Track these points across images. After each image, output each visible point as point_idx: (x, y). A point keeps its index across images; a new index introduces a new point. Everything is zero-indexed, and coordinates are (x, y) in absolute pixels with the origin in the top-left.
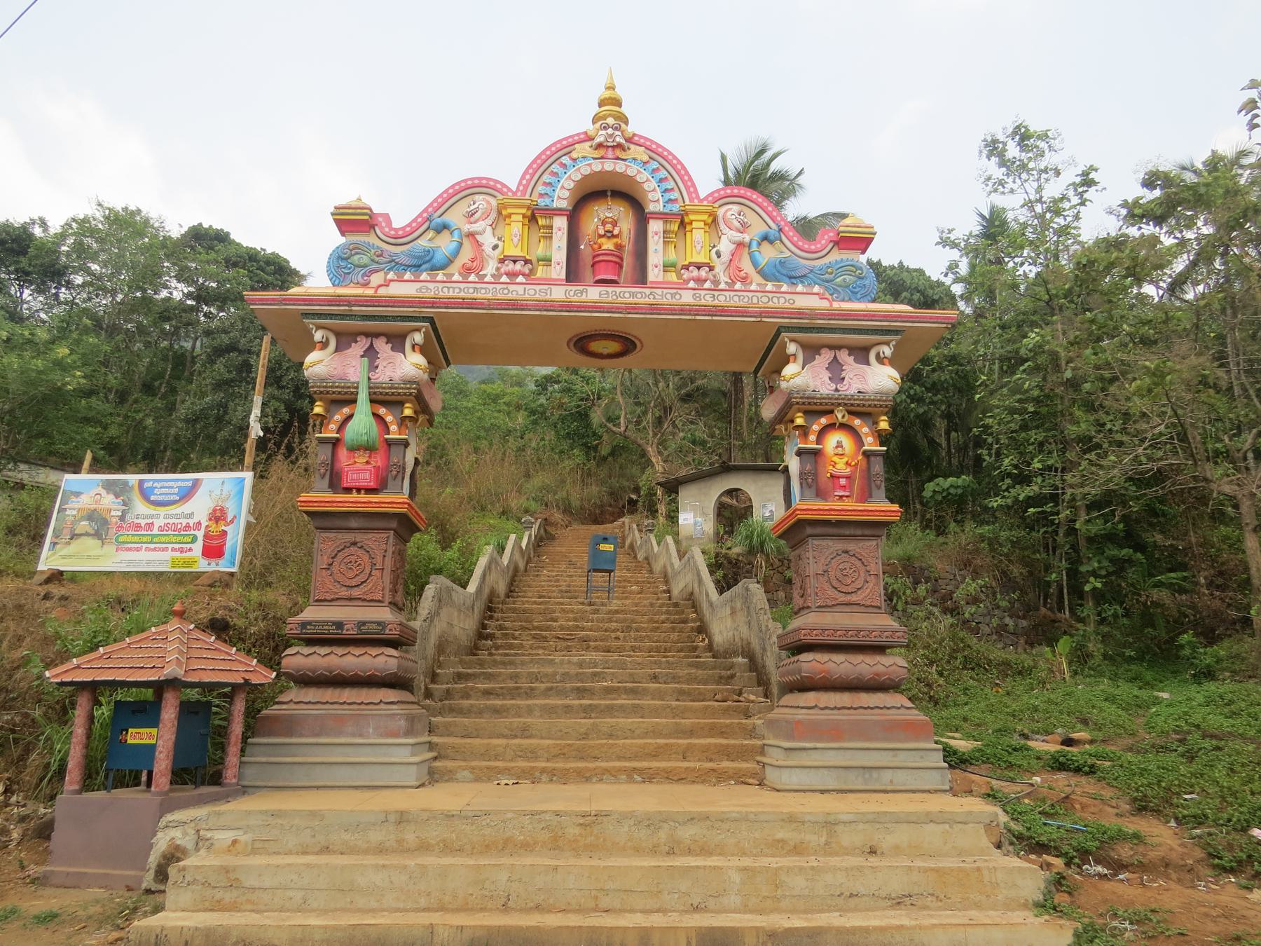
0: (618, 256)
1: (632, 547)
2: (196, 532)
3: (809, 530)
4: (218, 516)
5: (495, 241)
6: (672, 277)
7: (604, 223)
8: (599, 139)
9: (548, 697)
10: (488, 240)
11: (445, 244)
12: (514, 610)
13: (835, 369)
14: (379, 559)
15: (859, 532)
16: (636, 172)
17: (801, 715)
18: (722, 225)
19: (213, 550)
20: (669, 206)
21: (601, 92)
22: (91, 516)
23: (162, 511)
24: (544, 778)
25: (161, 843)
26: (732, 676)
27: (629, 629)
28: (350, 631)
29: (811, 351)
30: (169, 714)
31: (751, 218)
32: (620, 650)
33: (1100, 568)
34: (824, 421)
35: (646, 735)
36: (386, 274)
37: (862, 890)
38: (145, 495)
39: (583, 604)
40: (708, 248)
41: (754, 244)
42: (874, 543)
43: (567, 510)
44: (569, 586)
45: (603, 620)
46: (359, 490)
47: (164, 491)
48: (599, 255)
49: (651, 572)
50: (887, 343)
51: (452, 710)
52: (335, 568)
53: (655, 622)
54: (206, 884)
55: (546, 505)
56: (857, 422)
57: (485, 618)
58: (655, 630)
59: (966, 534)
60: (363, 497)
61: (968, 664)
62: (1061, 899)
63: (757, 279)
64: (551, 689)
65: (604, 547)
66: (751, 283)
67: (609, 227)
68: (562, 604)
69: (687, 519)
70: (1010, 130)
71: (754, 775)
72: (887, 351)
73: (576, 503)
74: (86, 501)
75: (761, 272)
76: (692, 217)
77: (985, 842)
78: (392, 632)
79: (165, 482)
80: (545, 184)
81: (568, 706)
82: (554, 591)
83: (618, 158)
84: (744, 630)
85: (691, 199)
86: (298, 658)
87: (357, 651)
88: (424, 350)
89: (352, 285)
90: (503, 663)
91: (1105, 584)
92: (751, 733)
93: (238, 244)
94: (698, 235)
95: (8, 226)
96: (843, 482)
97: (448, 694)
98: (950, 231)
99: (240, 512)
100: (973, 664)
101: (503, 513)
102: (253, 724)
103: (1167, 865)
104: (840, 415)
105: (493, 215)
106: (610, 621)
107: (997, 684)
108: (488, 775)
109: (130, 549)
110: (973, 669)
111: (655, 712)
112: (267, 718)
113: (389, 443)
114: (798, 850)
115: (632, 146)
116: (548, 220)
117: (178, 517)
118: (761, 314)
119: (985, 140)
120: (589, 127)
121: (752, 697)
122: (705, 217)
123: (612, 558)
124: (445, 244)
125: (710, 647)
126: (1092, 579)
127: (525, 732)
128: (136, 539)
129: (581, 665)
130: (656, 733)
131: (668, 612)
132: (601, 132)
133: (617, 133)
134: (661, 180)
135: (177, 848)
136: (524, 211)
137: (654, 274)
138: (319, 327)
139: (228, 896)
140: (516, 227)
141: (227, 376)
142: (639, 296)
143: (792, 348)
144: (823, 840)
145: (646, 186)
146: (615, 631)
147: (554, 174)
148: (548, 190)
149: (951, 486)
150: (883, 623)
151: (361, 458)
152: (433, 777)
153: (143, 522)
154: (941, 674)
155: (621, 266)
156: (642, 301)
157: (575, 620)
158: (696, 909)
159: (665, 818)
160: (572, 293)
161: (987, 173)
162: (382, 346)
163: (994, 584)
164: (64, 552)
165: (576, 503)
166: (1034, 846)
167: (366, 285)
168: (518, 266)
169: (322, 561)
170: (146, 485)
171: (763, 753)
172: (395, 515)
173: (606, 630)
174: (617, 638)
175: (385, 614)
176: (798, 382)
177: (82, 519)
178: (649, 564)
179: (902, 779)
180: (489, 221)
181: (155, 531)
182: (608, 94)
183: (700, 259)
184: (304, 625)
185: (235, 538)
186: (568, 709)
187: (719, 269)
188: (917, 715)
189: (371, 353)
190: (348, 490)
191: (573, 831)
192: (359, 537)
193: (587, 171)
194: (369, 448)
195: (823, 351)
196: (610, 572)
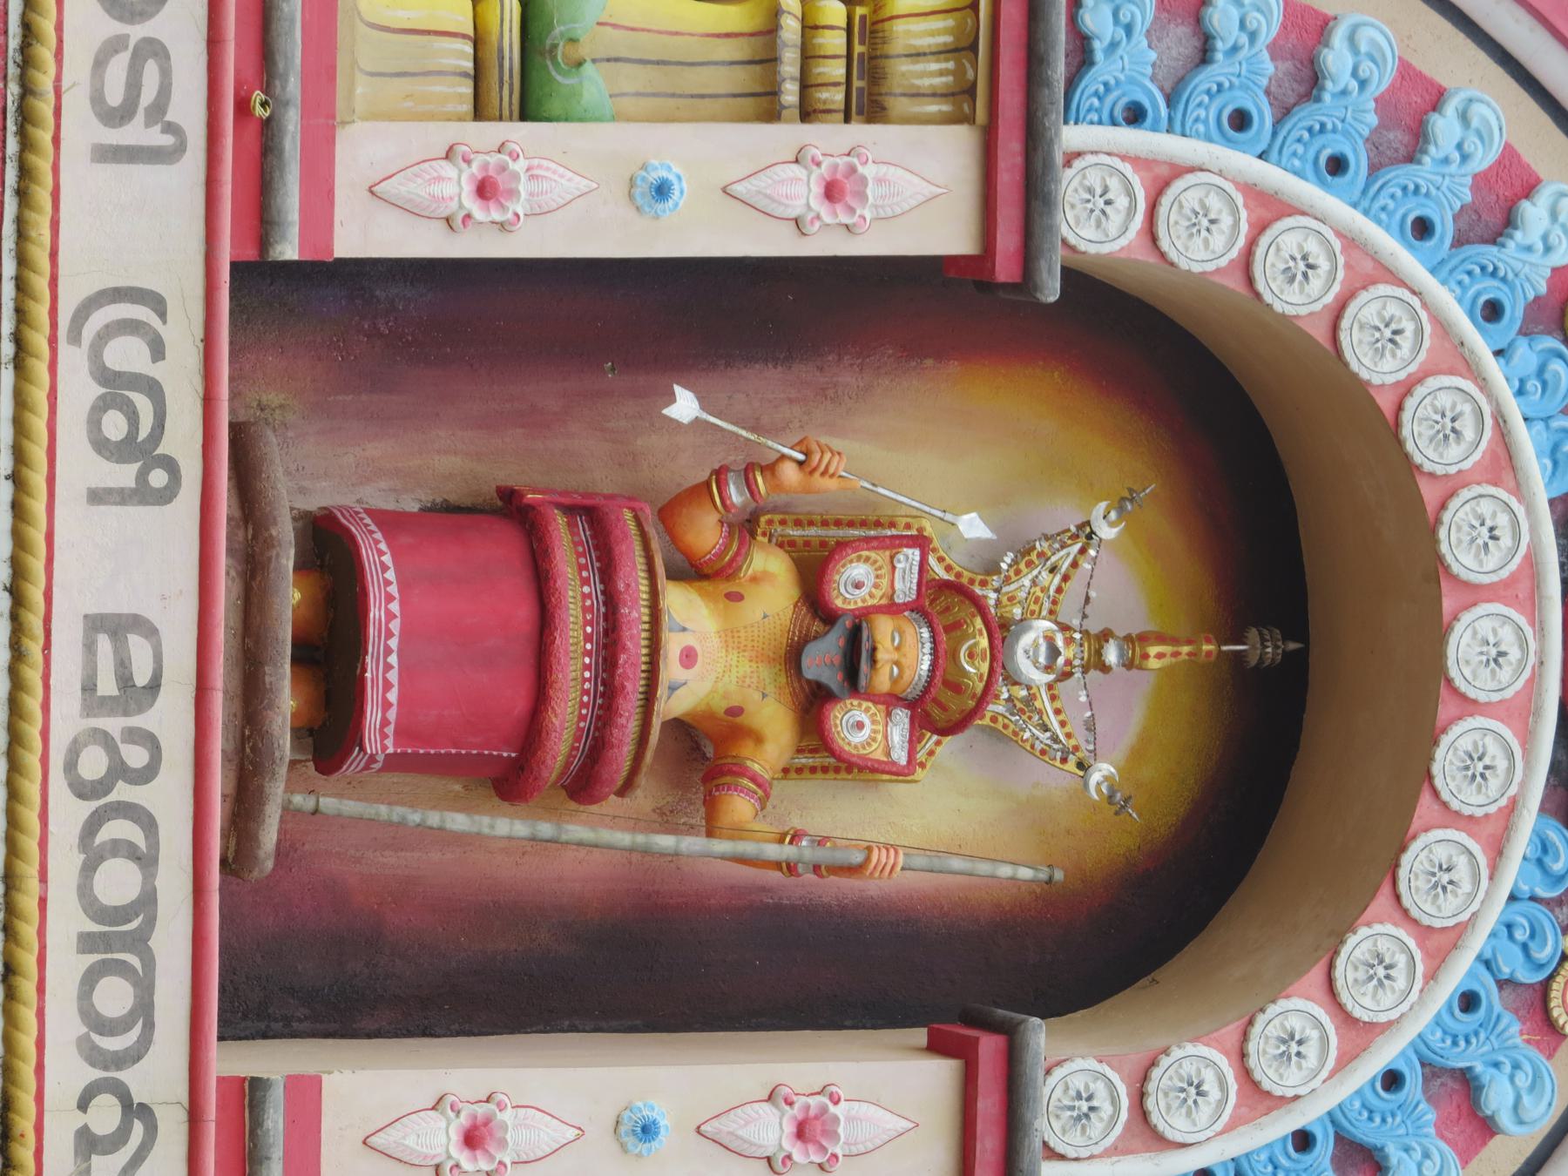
0: (596, 747)
16: (1439, 912)
48: (607, 568)
116: (933, 74)
142: (114, 997)
156: (64, 1025)
160: (127, 355)
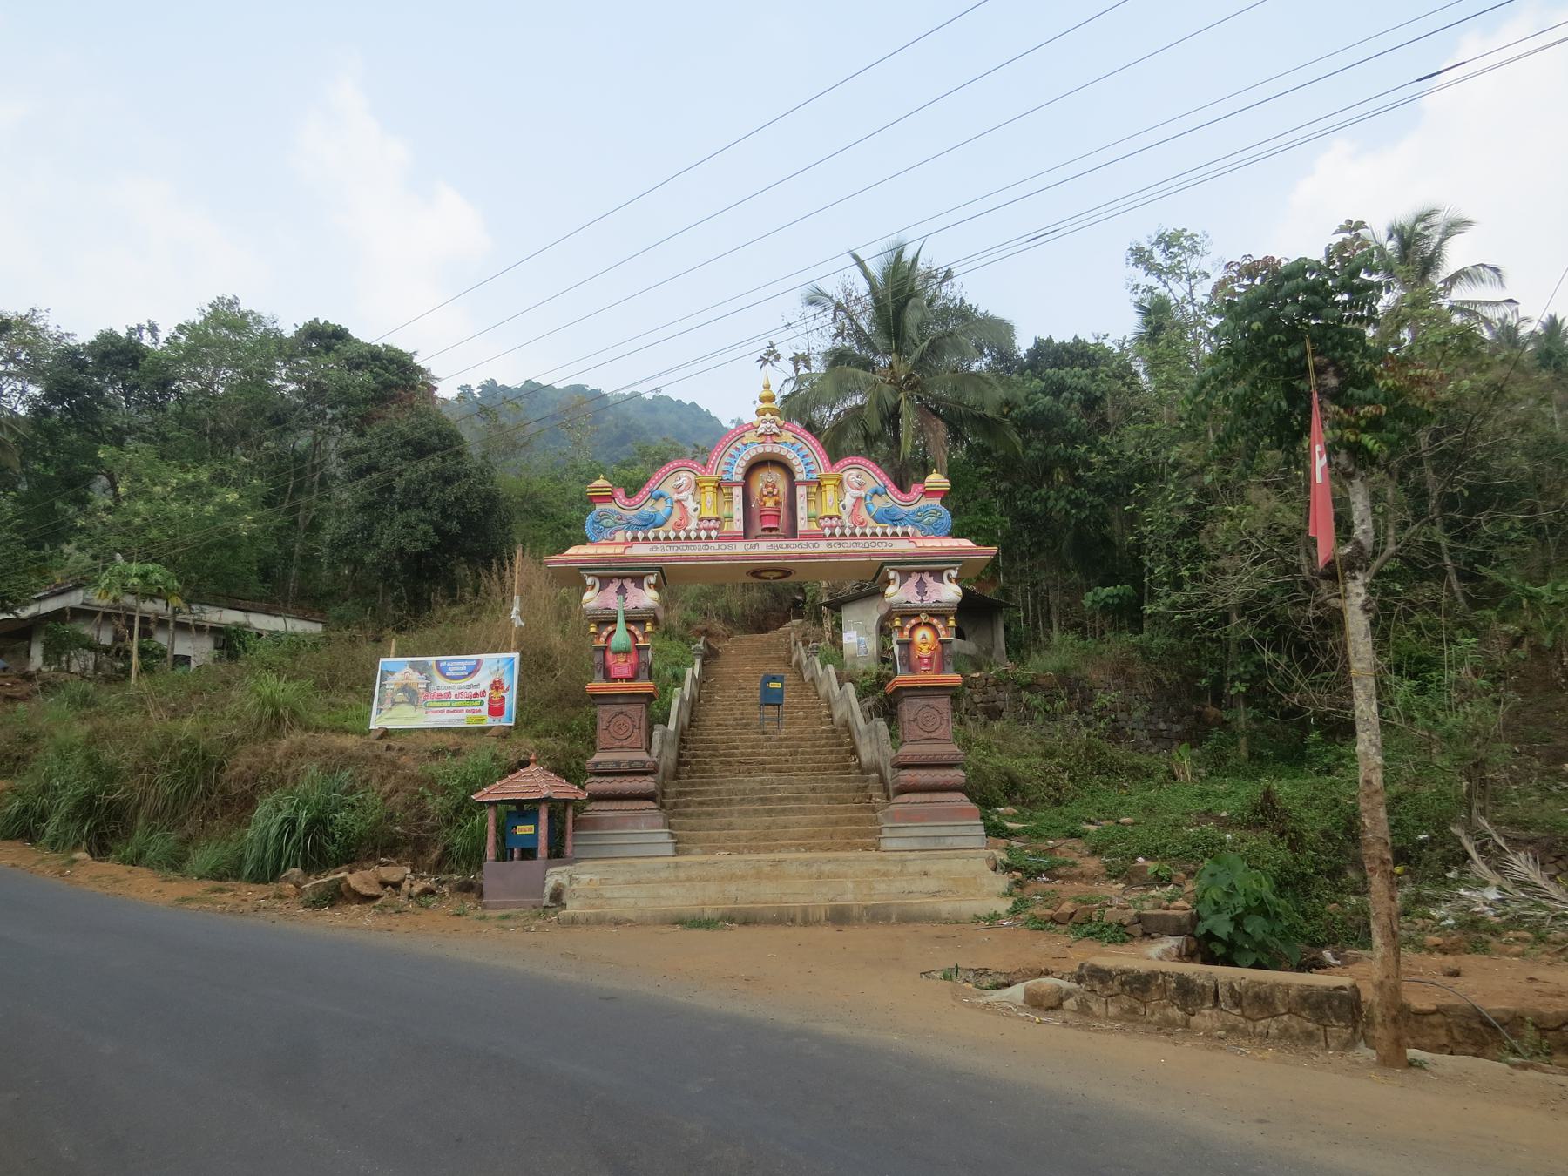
1: (798, 664)
2: (483, 698)
3: (904, 693)
4: (497, 686)
5: (695, 505)
6: (814, 526)
7: (766, 486)
8: (760, 431)
9: (742, 805)
10: (690, 505)
11: (662, 508)
12: (702, 741)
13: (921, 585)
14: (638, 722)
15: (936, 693)
17: (899, 807)
18: (846, 486)
19: (496, 711)
20: (810, 475)
21: (760, 391)
22: (405, 688)
23: (457, 683)
24: (745, 851)
25: (551, 883)
26: (866, 787)
27: (796, 753)
28: (624, 767)
29: (905, 575)
30: (544, 816)
31: (866, 478)
32: (789, 770)
33: (1245, 672)
34: (913, 622)
35: (807, 826)
36: (626, 533)
37: (915, 890)
38: (442, 672)
39: (757, 733)
40: (837, 502)
41: (868, 501)
42: (946, 699)
43: (727, 619)
44: (742, 714)
45: (775, 747)
46: (621, 679)
47: (458, 669)
49: (816, 693)
50: (954, 569)
51: (680, 815)
52: (611, 729)
53: (818, 746)
54: (586, 897)
55: (706, 614)
56: (935, 621)
57: (680, 748)
58: (816, 753)
59: (1120, 644)
60: (625, 684)
61: (1100, 769)
62: (1016, 890)
63: (872, 523)
64: (743, 799)
65: (773, 685)
66: (866, 527)
67: (770, 489)
68: (740, 734)
69: (850, 638)
70: (1155, 238)
71: (873, 845)
72: (954, 574)
73: (736, 608)
74: (399, 677)
75: (873, 517)
76: (825, 482)
77: (986, 868)
78: (649, 767)
79: (457, 662)
80: (727, 464)
81: (756, 810)
82: (727, 720)
83: (775, 443)
84: (876, 754)
85: (825, 470)
86: (596, 785)
87: (630, 779)
88: (657, 587)
89: (604, 541)
90: (708, 783)
91: (1248, 689)
92: (876, 821)
93: (357, 341)
94: (830, 494)
95: (112, 335)
96: (926, 661)
97: (675, 805)
98: (1105, 337)
99: (512, 681)
100: (1108, 770)
101: (666, 632)
102: (578, 824)
103: (1083, 876)
104: (923, 618)
105: (693, 486)
106: (781, 747)
107: (1125, 787)
108: (712, 851)
109: (436, 712)
110: (1106, 774)
111: (813, 812)
112: (582, 819)
113: (639, 649)
114: (885, 874)
115: (784, 433)
117: (469, 687)
118: (870, 556)
119: (1131, 249)
120: (754, 419)
121: (878, 800)
122: (834, 482)
123: (779, 694)
124: (662, 508)
125: (859, 766)
126: (1237, 684)
127: (730, 826)
128: (439, 704)
129: (762, 782)
130: (813, 824)
131: (827, 738)
132: (762, 425)
133: (774, 425)
134: (804, 457)
135: (560, 884)
136: (713, 484)
137: (802, 525)
138: (589, 576)
139: (598, 902)
140: (709, 496)
141: (370, 498)
143: (891, 575)
144: (899, 870)
145: (793, 462)
146: (786, 755)
147: (732, 456)
148: (729, 468)
149: (1108, 596)
150: (951, 750)
151: (621, 659)
152: (678, 852)
153: (443, 692)
154: (1072, 779)
155: (779, 516)
157: (753, 747)
158: (831, 901)
159: (815, 861)
161: (1135, 283)
162: (629, 585)
163: (1147, 691)
164: (387, 716)
165: (736, 608)
166: (1008, 868)
167: (612, 543)
168: (712, 524)
169: (602, 725)
170: (441, 665)
171: (881, 833)
172: (646, 694)
173: (778, 755)
174: (787, 761)
175: (643, 756)
176: (895, 598)
177: (399, 691)
178: (814, 685)
179: (959, 842)
180: (690, 491)
181: (453, 698)
182: (765, 393)
183: (832, 512)
184: (597, 764)
185: (511, 700)
186: (756, 812)
187: (845, 517)
188: (973, 806)
189: (622, 590)
190: (615, 680)
191: (767, 869)
192: (624, 709)
193: (753, 453)
194: (626, 652)
195: (913, 575)
196: (779, 705)
